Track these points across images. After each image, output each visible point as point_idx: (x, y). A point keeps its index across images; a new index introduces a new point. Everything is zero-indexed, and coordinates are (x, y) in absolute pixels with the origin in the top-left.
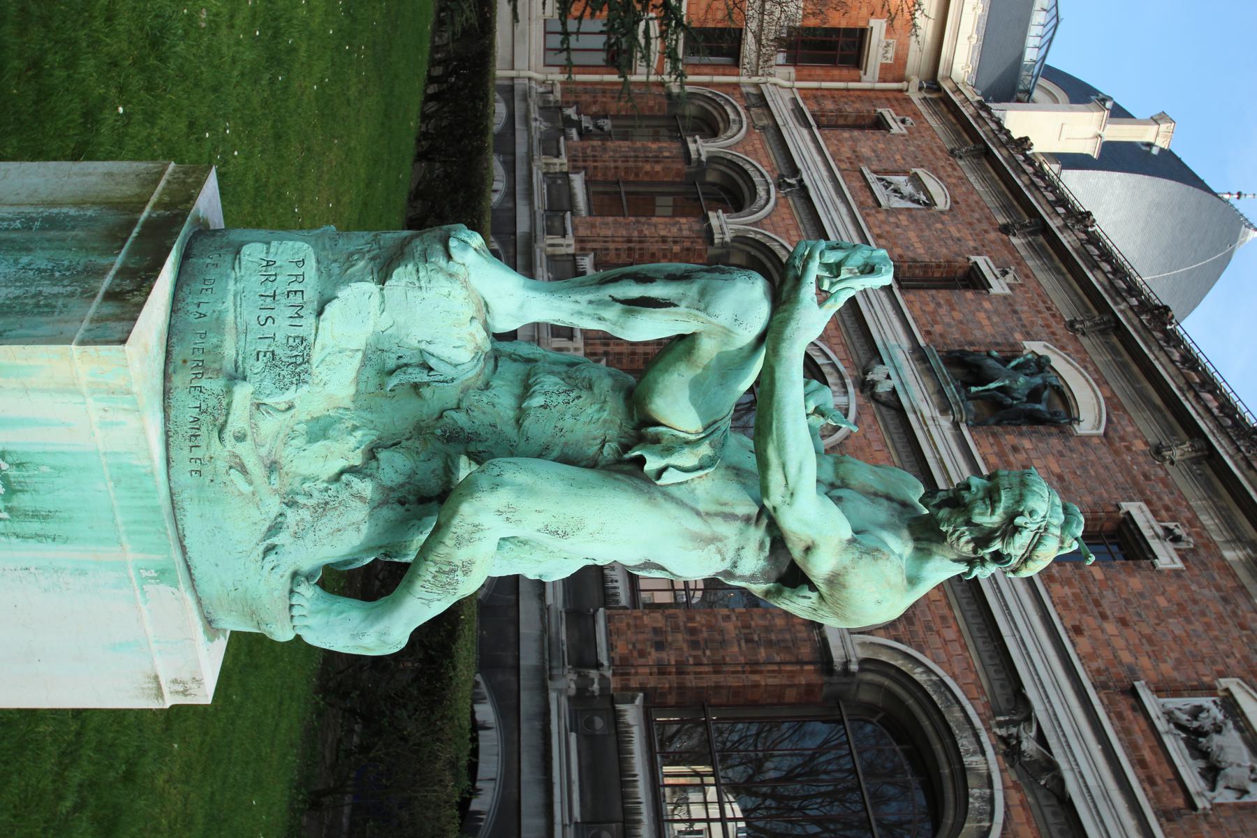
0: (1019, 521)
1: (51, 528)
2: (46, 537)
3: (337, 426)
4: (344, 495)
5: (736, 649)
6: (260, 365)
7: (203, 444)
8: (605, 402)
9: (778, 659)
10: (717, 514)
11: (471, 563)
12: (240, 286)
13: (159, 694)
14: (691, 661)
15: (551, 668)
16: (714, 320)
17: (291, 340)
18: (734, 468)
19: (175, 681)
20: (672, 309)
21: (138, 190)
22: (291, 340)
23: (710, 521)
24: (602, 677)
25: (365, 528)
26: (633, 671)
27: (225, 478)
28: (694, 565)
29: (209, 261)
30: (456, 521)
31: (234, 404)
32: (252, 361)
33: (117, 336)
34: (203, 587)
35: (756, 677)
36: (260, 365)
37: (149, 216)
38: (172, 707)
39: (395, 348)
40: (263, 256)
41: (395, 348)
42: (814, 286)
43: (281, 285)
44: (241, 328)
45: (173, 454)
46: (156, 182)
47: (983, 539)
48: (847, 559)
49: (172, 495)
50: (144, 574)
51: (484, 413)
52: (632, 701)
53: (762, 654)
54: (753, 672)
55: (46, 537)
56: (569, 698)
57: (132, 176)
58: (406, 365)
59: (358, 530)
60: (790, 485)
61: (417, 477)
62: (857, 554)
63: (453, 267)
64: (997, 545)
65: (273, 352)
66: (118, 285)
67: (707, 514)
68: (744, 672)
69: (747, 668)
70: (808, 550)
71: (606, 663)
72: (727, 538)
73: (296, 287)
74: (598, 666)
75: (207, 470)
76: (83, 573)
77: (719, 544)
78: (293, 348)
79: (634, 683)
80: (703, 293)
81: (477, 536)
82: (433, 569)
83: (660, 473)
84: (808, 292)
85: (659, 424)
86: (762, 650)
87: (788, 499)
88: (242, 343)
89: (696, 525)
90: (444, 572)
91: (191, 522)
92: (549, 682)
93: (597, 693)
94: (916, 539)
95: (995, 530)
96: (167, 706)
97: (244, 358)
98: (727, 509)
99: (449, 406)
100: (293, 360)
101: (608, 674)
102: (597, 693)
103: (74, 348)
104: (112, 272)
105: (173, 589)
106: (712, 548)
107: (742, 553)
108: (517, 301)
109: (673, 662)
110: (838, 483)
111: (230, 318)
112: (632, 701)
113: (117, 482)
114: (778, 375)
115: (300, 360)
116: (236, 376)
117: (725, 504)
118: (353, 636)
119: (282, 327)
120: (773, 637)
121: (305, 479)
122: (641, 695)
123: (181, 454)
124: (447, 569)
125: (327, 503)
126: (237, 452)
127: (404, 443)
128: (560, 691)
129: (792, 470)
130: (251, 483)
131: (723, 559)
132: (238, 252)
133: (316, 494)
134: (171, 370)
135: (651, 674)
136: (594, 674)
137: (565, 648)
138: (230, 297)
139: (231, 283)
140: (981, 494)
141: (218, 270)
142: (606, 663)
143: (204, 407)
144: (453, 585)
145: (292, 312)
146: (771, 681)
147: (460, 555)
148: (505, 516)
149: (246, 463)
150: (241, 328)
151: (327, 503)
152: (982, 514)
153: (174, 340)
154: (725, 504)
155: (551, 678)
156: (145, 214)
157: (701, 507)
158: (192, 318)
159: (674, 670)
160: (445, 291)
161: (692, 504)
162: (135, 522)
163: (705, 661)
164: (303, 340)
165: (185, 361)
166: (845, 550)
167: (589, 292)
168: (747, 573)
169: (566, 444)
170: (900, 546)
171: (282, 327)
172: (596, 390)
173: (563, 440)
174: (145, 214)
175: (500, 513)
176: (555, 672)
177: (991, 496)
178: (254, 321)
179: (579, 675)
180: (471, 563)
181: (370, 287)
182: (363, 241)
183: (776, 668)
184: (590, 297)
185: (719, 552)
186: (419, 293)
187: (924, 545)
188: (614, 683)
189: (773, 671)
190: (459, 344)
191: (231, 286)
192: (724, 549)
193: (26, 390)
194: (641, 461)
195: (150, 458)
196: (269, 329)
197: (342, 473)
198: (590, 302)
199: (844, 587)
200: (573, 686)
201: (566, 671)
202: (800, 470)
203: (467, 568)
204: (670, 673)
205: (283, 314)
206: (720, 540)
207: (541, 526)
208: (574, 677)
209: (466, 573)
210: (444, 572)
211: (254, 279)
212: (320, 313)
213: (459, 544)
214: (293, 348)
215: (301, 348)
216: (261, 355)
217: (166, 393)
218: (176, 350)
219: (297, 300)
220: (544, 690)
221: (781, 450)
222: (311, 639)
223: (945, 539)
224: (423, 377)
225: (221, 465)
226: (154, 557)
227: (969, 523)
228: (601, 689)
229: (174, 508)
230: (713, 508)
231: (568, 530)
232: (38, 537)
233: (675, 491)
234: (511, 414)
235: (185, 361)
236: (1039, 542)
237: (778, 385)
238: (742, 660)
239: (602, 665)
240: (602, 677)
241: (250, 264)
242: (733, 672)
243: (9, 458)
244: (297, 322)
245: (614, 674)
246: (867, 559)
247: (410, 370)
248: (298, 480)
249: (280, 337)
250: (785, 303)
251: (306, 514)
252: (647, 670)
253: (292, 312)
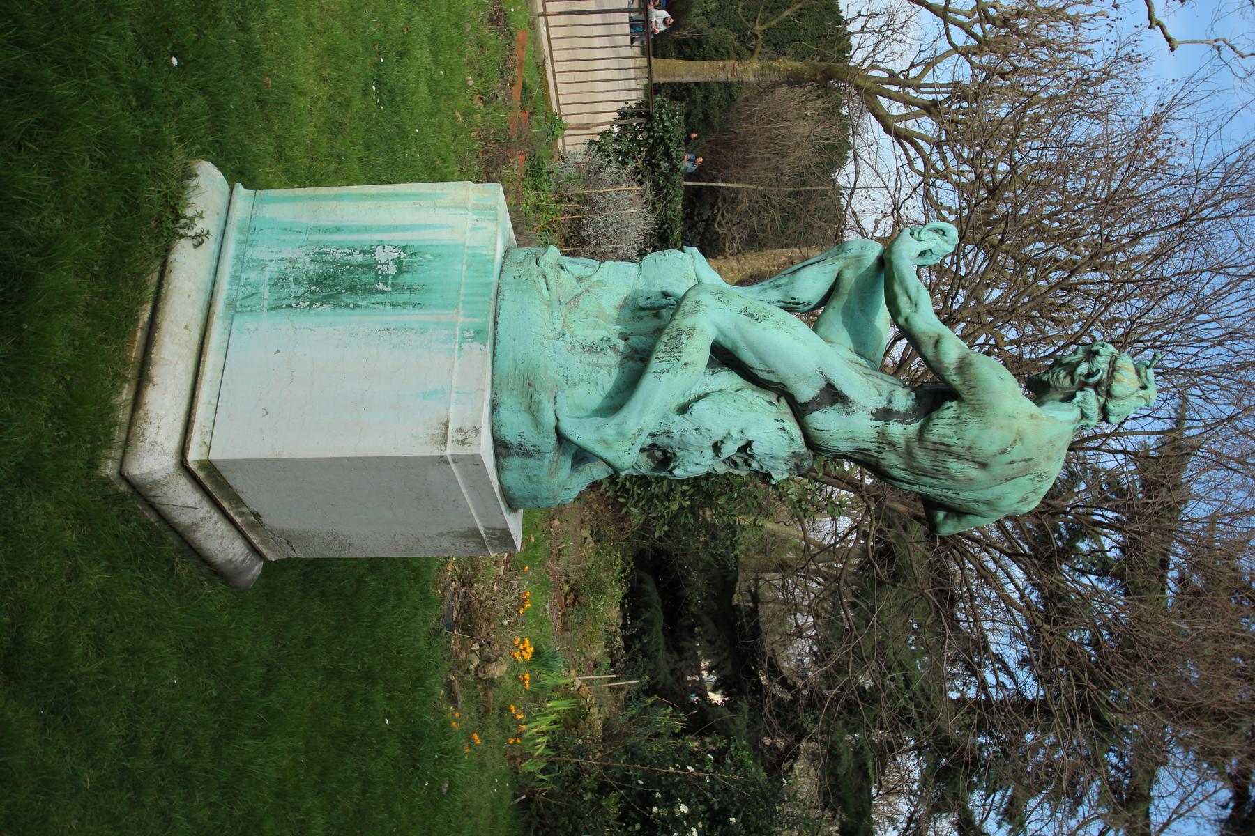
1: (415, 298)
2: (410, 304)
16: (849, 254)
25: (615, 372)
55: (410, 304)
59: (610, 373)
70: (937, 343)
76: (423, 331)
91: (507, 305)
113: (469, 266)
123: (510, 271)
162: (471, 295)
193: (435, 207)
195: (495, 250)
199: (970, 365)
207: (741, 308)
213: (685, 315)
224: (664, 301)
226: (477, 320)
232: (405, 305)
243: (408, 250)
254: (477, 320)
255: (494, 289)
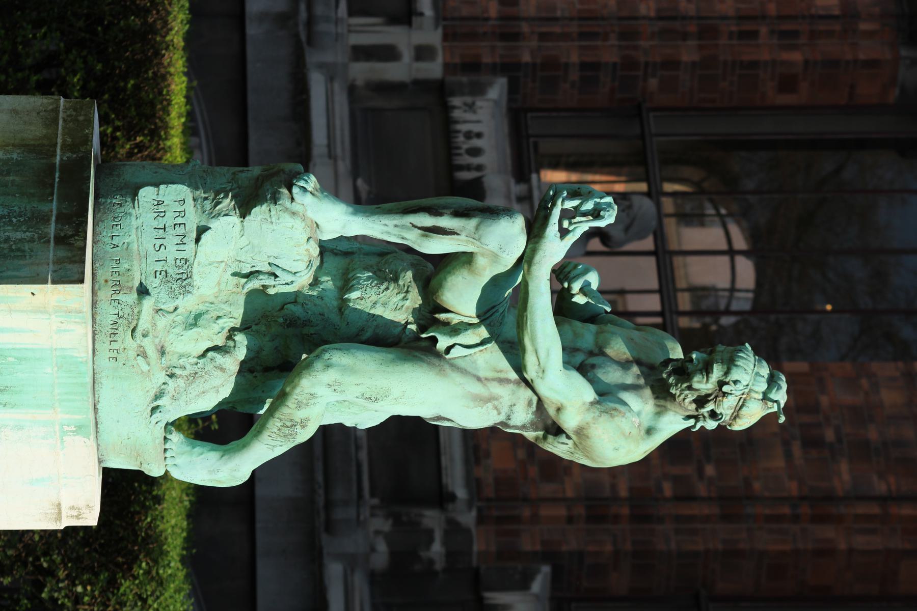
0: (725, 389)
3: (205, 316)
4: (210, 367)
5: (779, 463)
6: (157, 281)
7: (120, 340)
8: (407, 292)
9: (880, 487)
10: (494, 380)
11: (308, 420)
12: (139, 221)
13: (59, 518)
14: (668, 489)
15: (329, 505)
17: (178, 261)
18: (509, 342)
19: (72, 508)
20: (455, 237)
21: (45, 131)
22: (178, 261)
23: (489, 384)
24: (453, 528)
26: (526, 512)
27: (134, 363)
28: (477, 419)
29: (114, 201)
30: (298, 390)
31: (143, 313)
32: (152, 278)
33: (76, 277)
34: (104, 436)
35: (828, 532)
36: (157, 281)
37: (61, 159)
38: (67, 528)
39: (249, 260)
40: (155, 197)
41: (249, 260)
42: (557, 225)
43: (169, 220)
44: (143, 254)
45: (97, 346)
46: (55, 121)
47: (701, 401)
48: (589, 417)
49: (94, 374)
50: (66, 428)
51: (315, 305)
52: (523, 584)
53: (844, 475)
54: (819, 519)
56: (373, 578)
57: (34, 114)
58: (257, 272)
60: (542, 365)
61: (264, 353)
62: (598, 413)
63: (295, 207)
64: (710, 406)
65: (166, 272)
66: (61, 230)
67: (486, 379)
68: (796, 518)
69: (805, 510)
70: (559, 410)
71: (461, 493)
72: (501, 397)
73: (179, 220)
74: (443, 499)
75: (121, 358)
76: (20, 428)
77: (496, 403)
78: (180, 267)
79: (527, 544)
80: (477, 228)
81: (312, 401)
82: (279, 424)
83: (448, 350)
84: (552, 229)
85: (447, 311)
86: (844, 467)
87: (540, 374)
88: (144, 265)
89: (477, 388)
90: (287, 427)
92: (325, 538)
93: (439, 566)
94: (657, 398)
95: (710, 395)
96: (62, 528)
97: (146, 277)
98: (502, 375)
99: (289, 301)
100: (180, 276)
101: (468, 518)
102: (439, 566)
103: (49, 287)
104: (54, 218)
105: (86, 440)
106: (490, 405)
107: (514, 408)
108: (339, 220)
109: (623, 493)
110: (596, 351)
111: (135, 247)
112: (523, 584)
114: (530, 288)
115: (185, 276)
116: (143, 291)
117: (501, 371)
118: (210, 472)
119: (171, 252)
120: (873, 434)
121: (181, 356)
122: (546, 569)
123: (104, 347)
124: (289, 424)
125: (196, 373)
126: (143, 344)
127: (254, 328)
128: (351, 562)
129: (542, 355)
130: (149, 364)
131: (499, 414)
132: (136, 194)
133: (188, 366)
134: (97, 287)
135: (570, 520)
136: (432, 518)
137: (363, 455)
138: (134, 231)
139: (133, 218)
140: (700, 366)
141: (123, 209)
142: (461, 493)
143: (121, 314)
144: (293, 435)
145: (178, 240)
146: (861, 541)
147: (300, 415)
148: (333, 388)
149: (147, 351)
150: (143, 254)
151: (196, 373)
152: (699, 382)
153: (97, 265)
154: (501, 371)
155: (329, 527)
156: (58, 158)
157: (482, 374)
158: (108, 248)
159: (625, 511)
160: (290, 225)
161: (475, 372)
163: (702, 489)
164: (186, 261)
165: (106, 281)
166: (588, 410)
167: (395, 219)
168: (519, 424)
169: (377, 326)
170: (641, 405)
171: (171, 252)
172: (401, 282)
173: (375, 323)
174: (58, 158)
175: (330, 385)
176: (339, 514)
177: (707, 369)
178: (151, 249)
179: (397, 520)
180: (308, 420)
181: (235, 219)
182: (225, 180)
183: (875, 509)
184: (395, 222)
185: (496, 408)
186: (271, 226)
187: (662, 402)
188: (481, 544)
189: (868, 518)
190: (298, 258)
191: (134, 223)
192: (500, 406)
193: (10, 311)
194: (434, 340)
195: (88, 352)
196: (162, 254)
197: (208, 350)
198: (396, 226)
199: (588, 437)
200: (382, 547)
201: (365, 512)
202: (548, 355)
203: (303, 424)
204: (617, 518)
205: (171, 241)
206: (496, 399)
207: (359, 394)
208: (385, 525)
209: (303, 427)
210: (287, 427)
211: (149, 215)
212: (198, 240)
213: (299, 406)
214: (180, 267)
215: (185, 267)
216: (158, 273)
217: (94, 304)
218: (99, 273)
219: (180, 230)
220: (314, 558)
221: (533, 340)
222: (176, 474)
223: (675, 400)
225: (132, 354)
226: (76, 417)
227: (690, 388)
228: (451, 555)
229: (94, 383)
230: (491, 374)
231: (379, 397)
233: (460, 363)
234: (335, 303)
235: (106, 281)
236: (742, 406)
237: (531, 295)
238: (793, 488)
239: (452, 497)
240: (453, 528)
241: (145, 204)
242: (770, 519)
244: (182, 247)
245: (481, 520)
246: (605, 417)
247: (261, 277)
248: (176, 356)
249: (171, 261)
250: (536, 237)
251: (181, 382)
252: (562, 511)
253: (178, 240)
254: (76, 417)
255: (89, 379)
